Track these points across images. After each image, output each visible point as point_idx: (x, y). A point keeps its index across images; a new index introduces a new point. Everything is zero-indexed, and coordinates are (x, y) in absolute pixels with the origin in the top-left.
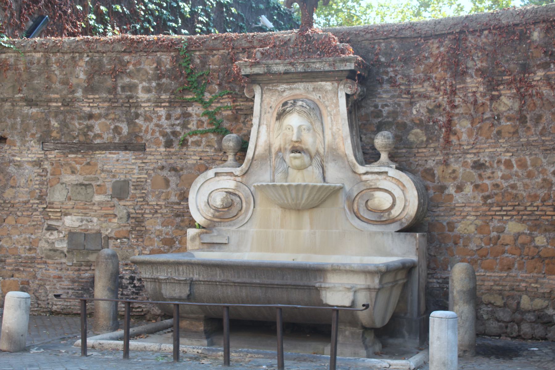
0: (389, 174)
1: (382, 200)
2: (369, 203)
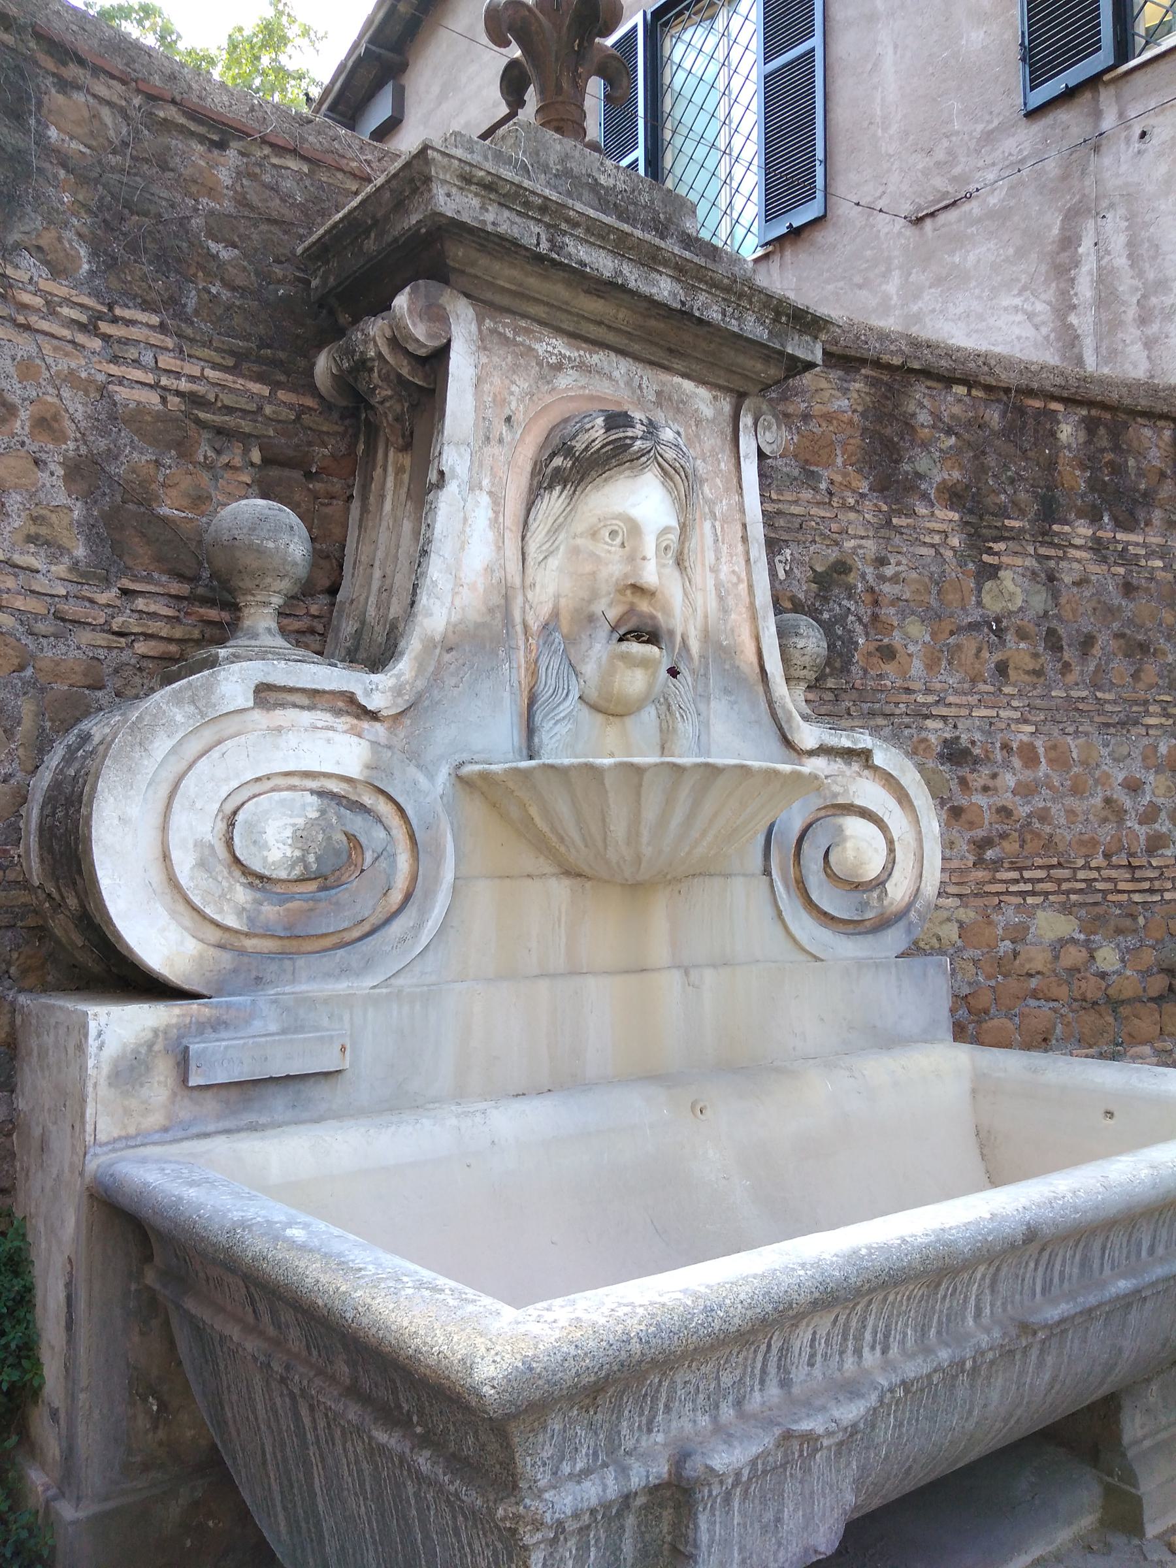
0: (879, 759)
1: (861, 846)
2: (832, 858)
